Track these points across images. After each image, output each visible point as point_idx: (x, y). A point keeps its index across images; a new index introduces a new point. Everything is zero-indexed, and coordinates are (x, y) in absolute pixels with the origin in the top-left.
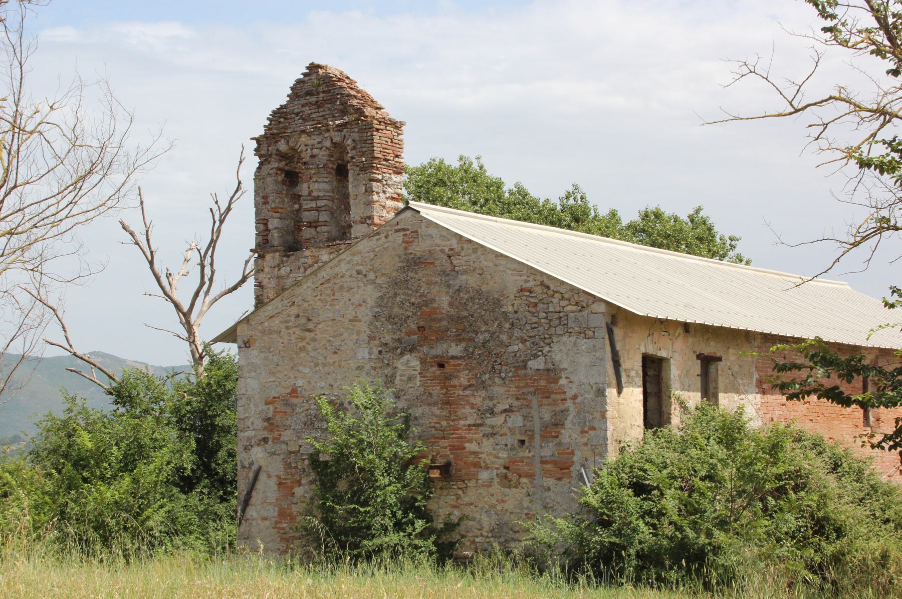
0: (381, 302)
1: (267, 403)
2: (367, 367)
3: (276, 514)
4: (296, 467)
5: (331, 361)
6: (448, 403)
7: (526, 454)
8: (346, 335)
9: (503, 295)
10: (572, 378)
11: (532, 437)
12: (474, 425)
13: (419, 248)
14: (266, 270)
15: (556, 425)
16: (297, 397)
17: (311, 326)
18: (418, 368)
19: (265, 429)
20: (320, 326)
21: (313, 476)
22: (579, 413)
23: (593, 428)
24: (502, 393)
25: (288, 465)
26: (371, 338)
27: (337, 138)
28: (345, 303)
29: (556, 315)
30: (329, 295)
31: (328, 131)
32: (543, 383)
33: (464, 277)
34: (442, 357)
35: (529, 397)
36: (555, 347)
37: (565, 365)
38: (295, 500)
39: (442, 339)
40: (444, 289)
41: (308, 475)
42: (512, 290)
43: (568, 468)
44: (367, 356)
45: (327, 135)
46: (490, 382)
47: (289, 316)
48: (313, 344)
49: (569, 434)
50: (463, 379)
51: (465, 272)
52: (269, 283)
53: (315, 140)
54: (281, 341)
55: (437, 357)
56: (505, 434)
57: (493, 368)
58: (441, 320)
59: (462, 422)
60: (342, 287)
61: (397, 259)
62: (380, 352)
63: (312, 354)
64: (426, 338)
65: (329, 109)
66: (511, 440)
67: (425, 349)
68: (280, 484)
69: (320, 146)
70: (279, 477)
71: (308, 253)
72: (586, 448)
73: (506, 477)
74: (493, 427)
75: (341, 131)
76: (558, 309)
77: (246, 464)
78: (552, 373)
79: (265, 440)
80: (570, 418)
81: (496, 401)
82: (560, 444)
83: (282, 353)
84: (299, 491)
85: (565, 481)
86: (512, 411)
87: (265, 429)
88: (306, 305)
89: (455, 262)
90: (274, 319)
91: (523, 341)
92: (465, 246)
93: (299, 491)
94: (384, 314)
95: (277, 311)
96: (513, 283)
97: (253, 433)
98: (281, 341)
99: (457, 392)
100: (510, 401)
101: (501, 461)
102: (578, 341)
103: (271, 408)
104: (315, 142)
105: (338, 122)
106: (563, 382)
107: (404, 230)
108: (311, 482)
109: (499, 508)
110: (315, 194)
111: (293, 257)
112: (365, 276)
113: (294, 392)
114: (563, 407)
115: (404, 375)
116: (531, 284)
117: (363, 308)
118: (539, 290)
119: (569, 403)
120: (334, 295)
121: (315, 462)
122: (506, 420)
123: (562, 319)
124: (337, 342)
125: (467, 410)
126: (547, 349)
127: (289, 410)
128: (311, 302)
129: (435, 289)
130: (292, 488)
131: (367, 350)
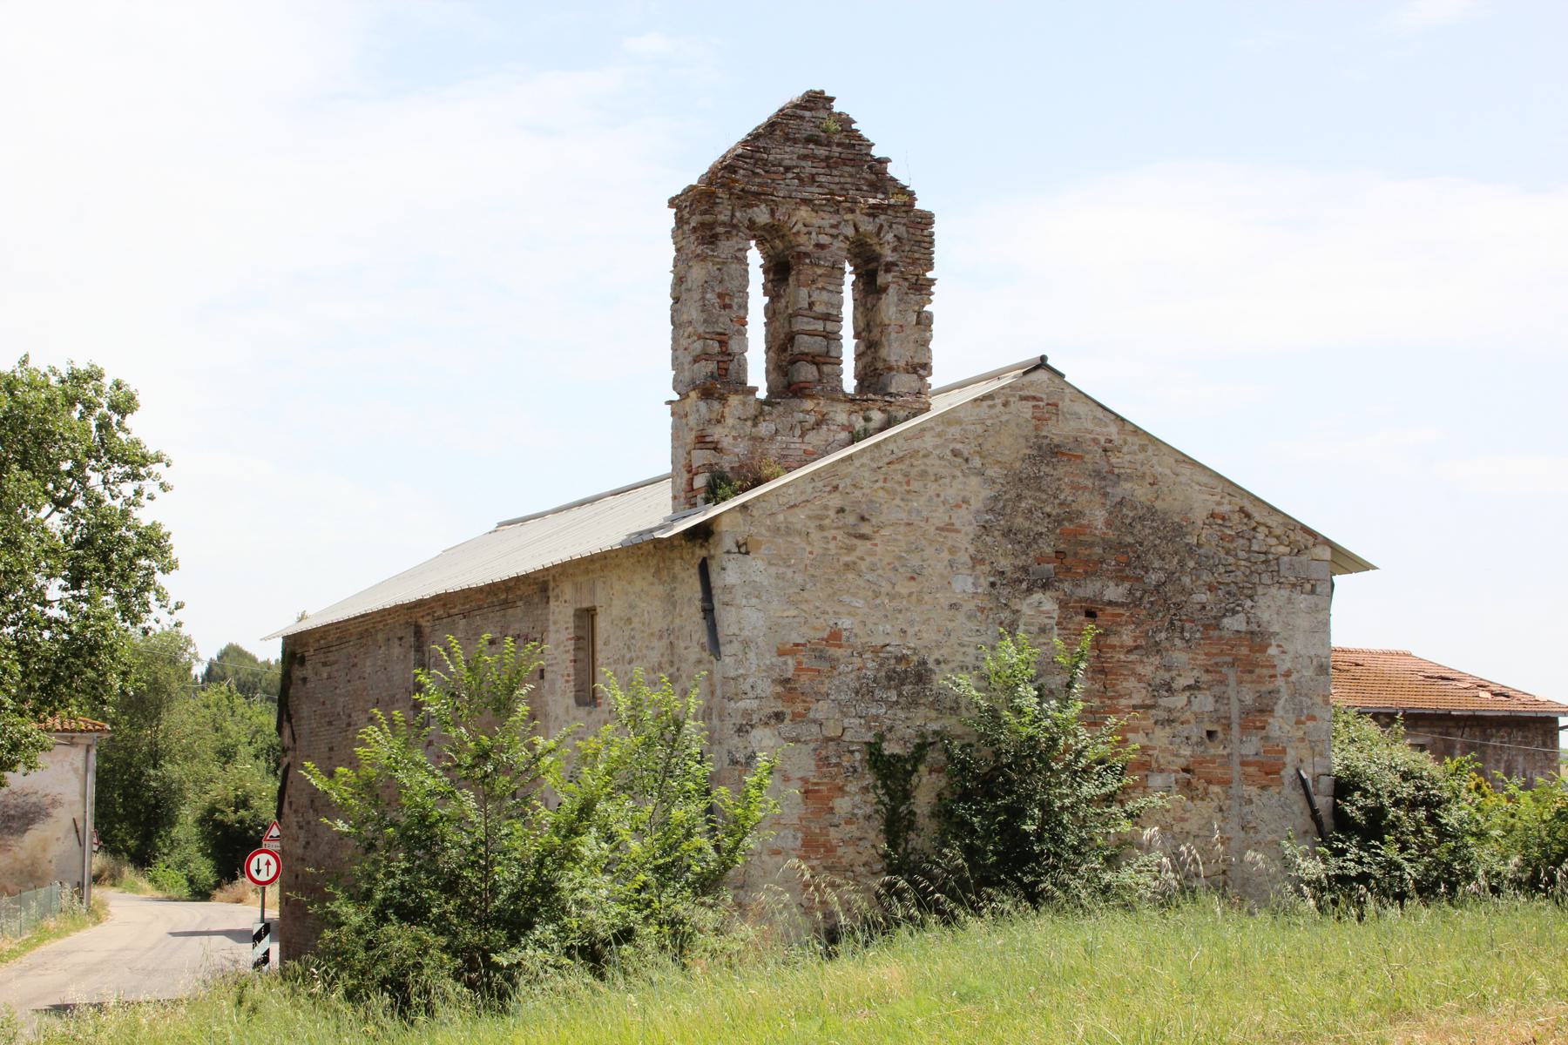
0: (994, 506)
1: (781, 653)
2: (970, 606)
3: (799, 842)
4: (837, 765)
5: (904, 591)
6: (1102, 671)
7: (1220, 751)
8: (929, 552)
9: (1187, 520)
10: (1286, 646)
11: (1228, 727)
12: (1142, 707)
13: (1058, 431)
14: (730, 421)
15: (1261, 711)
16: (840, 646)
17: (865, 529)
18: (1055, 615)
19: (778, 696)
20: (883, 532)
21: (869, 779)
22: (1293, 696)
23: (1313, 718)
24: (1185, 662)
25: (824, 761)
26: (976, 561)
27: (867, 226)
28: (930, 500)
29: (1262, 557)
30: (900, 483)
31: (852, 211)
32: (1244, 651)
33: (1128, 486)
34: (1093, 601)
35: (1224, 670)
36: (1262, 602)
37: (1275, 628)
38: (836, 821)
39: (1094, 573)
40: (1098, 499)
41: (863, 777)
42: (1200, 515)
43: (1277, 773)
44: (970, 589)
45: (848, 217)
46: (1166, 644)
47: (826, 508)
48: (869, 559)
49: (1280, 724)
50: (1127, 636)
51: (1129, 478)
52: (735, 446)
53: (827, 220)
54: (809, 549)
55: (1086, 600)
56: (1188, 722)
57: (1172, 623)
58: (1092, 545)
59: (1123, 702)
60: (923, 474)
61: (1022, 441)
62: (993, 585)
63: (868, 577)
64: (1069, 570)
65: (851, 176)
66: (1197, 732)
67: (1067, 586)
68: (806, 792)
69: (835, 232)
70: (804, 780)
71: (809, 404)
72: (1301, 745)
73: (1189, 783)
74: (1170, 711)
75: (874, 216)
76: (1264, 549)
77: (740, 756)
78: (1257, 638)
79: (779, 717)
80: (1281, 702)
81: (1174, 673)
82: (1266, 738)
83: (811, 571)
84: (842, 805)
85: (1274, 790)
86: (1199, 689)
87: (778, 696)
88: (858, 493)
89: (1113, 460)
90: (796, 510)
91: (1211, 588)
92: (1129, 439)
93: (842, 805)
94: (998, 522)
95: (804, 498)
96: (1202, 504)
97: (755, 704)
98: (809, 549)
99: (1117, 656)
100: (1196, 673)
101: (1182, 762)
102: (1294, 596)
103: (791, 662)
104: (826, 223)
105: (871, 201)
106: (1272, 651)
107: (1034, 398)
108: (865, 790)
109: (1177, 829)
110: (819, 308)
111: (781, 409)
112: (967, 460)
113: (835, 637)
114: (1270, 687)
115: (1032, 624)
116: (1225, 508)
117: (963, 512)
118: (1236, 517)
119: (1280, 682)
120: (908, 483)
121: (876, 758)
122: (1189, 701)
123: (1269, 563)
124: (915, 561)
125: (1131, 683)
126: (1249, 603)
127: (825, 666)
128: (867, 491)
129: (1083, 498)
130: (830, 798)
131: (970, 580)
